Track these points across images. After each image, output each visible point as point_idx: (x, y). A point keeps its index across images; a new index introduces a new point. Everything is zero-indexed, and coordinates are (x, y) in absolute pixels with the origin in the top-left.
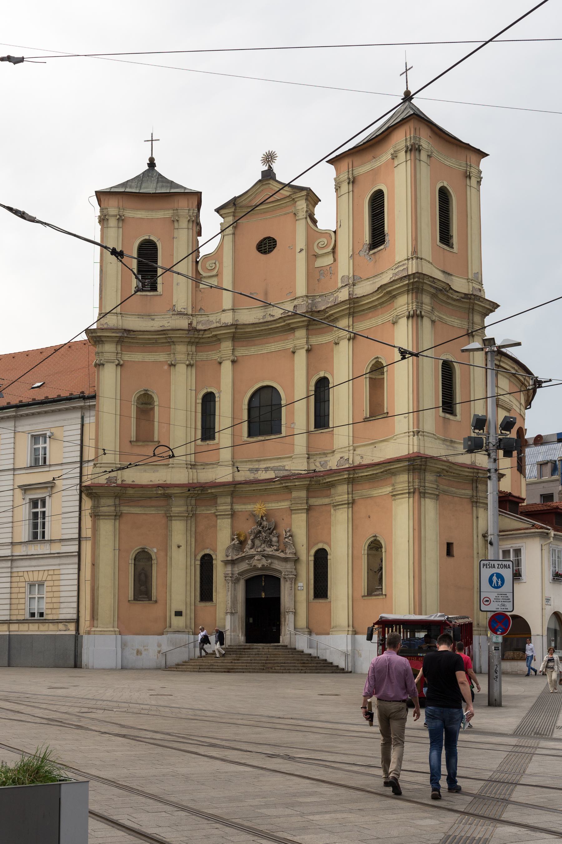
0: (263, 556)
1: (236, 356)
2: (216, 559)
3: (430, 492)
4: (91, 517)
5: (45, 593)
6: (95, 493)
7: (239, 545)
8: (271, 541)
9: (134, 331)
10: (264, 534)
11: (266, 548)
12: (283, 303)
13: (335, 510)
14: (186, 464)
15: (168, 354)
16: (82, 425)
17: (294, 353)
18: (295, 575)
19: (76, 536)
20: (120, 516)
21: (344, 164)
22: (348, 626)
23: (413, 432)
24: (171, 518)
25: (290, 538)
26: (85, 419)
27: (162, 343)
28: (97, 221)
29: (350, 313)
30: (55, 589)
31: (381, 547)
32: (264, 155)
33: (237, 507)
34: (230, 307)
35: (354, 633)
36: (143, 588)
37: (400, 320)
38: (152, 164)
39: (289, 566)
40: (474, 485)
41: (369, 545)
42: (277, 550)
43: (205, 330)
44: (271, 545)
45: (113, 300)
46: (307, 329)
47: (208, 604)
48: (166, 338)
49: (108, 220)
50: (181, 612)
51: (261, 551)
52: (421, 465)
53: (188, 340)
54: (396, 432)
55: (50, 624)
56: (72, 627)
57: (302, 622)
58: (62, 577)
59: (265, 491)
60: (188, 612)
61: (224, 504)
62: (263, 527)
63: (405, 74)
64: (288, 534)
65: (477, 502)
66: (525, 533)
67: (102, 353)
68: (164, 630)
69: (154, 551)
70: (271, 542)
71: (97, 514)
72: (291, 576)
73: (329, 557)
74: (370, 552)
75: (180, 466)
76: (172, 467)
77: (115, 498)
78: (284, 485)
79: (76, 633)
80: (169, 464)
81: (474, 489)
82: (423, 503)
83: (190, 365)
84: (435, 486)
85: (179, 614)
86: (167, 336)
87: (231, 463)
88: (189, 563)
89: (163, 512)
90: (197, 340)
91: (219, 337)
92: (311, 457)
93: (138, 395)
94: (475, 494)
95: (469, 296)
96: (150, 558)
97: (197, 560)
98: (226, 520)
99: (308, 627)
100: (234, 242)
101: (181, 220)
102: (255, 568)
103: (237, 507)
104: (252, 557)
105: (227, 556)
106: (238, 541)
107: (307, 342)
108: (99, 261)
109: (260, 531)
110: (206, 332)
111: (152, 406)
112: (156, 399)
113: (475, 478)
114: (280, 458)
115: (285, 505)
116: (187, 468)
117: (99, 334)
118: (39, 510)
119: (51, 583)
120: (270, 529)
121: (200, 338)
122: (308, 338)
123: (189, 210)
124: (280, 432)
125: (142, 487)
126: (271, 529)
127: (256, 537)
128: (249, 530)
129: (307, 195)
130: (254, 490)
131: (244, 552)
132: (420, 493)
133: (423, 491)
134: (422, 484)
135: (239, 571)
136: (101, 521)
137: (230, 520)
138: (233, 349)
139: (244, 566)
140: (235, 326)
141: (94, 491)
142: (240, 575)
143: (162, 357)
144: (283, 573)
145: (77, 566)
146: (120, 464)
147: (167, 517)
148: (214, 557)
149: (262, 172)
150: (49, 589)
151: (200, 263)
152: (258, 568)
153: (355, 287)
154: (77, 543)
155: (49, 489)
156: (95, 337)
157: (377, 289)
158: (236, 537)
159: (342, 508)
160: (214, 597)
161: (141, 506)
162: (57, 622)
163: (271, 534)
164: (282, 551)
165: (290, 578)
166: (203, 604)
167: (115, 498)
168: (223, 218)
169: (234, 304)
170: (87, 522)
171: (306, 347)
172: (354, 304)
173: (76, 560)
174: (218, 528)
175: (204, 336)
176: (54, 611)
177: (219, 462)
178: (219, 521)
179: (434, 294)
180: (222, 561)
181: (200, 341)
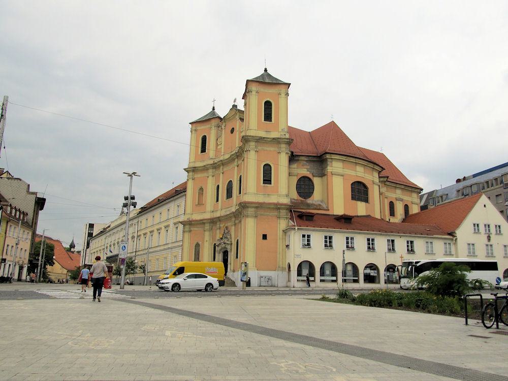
45: (193, 160)
69: (200, 243)
143: (205, 174)
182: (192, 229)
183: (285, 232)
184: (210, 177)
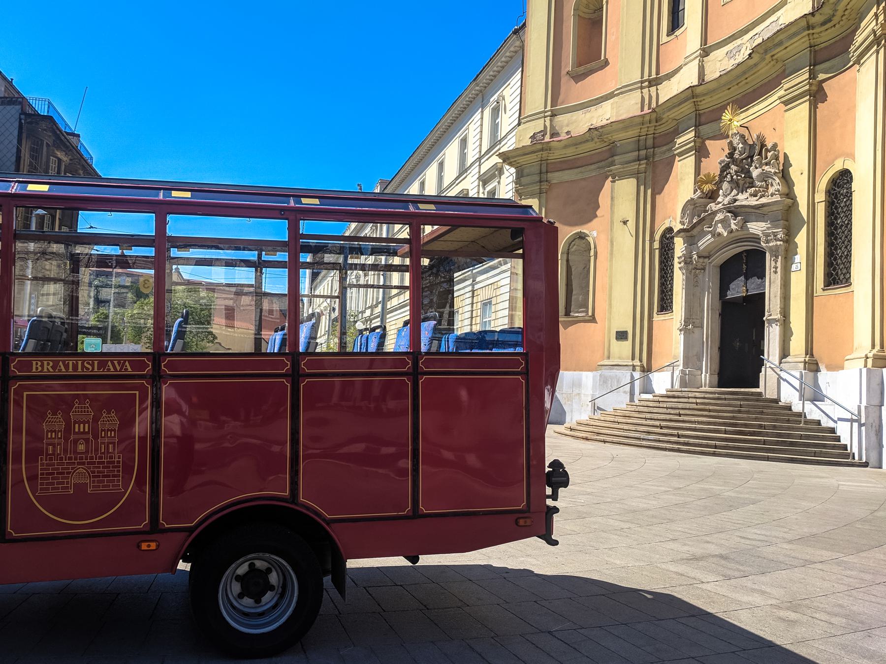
50: (626, 332)
85: (621, 336)
116: (642, 88)
166: (662, 317)
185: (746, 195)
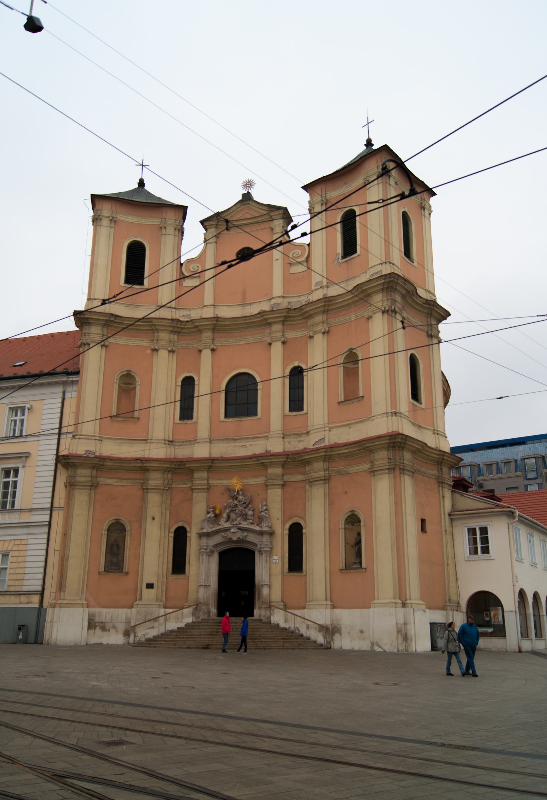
0: (238, 529)
1: (216, 346)
2: (190, 532)
3: (408, 469)
4: (66, 487)
5: (9, 563)
6: (73, 463)
7: (214, 518)
8: (246, 515)
9: (121, 317)
10: (240, 508)
11: (242, 522)
12: (260, 302)
13: (311, 486)
14: (165, 440)
15: (151, 340)
16: (63, 399)
17: (270, 344)
18: (271, 548)
19: (49, 506)
20: (96, 487)
21: (318, 189)
22: (326, 600)
23: (391, 413)
24: (147, 490)
25: (266, 511)
26: (66, 394)
27: (147, 330)
28: (91, 220)
29: (324, 310)
30: (20, 559)
31: (359, 521)
32: (244, 182)
33: (212, 482)
34: (211, 303)
35: (332, 606)
36: (114, 559)
37: (375, 315)
38: (141, 183)
39: (265, 538)
40: (439, 467)
41: (346, 520)
42: (252, 524)
43: (188, 321)
44: (246, 519)
46: (283, 324)
47: (181, 576)
48: (150, 325)
49: (101, 219)
51: (237, 524)
52: (401, 443)
53: (171, 329)
54: (373, 413)
55: (12, 597)
56: (36, 599)
57: (276, 595)
58: (29, 547)
59: (241, 467)
60: (160, 584)
61: (200, 478)
62: (239, 501)
63: (367, 126)
64: (265, 508)
65: (442, 483)
66: (492, 512)
67: (89, 333)
68: (135, 603)
70: (246, 516)
71: (73, 484)
72: (267, 549)
73: (304, 531)
74: (346, 526)
75: (158, 441)
76: (151, 443)
77: (92, 469)
78: (260, 461)
79: (40, 606)
80: (148, 440)
81: (440, 470)
82: (402, 479)
83: (171, 351)
84: (411, 464)
85: (150, 586)
86: (152, 324)
87: (208, 440)
88: (163, 535)
89: (139, 485)
90: (179, 330)
91: (200, 328)
92: (286, 437)
93: (121, 374)
94: (440, 475)
95: (430, 302)
96: (123, 529)
97: (171, 532)
98: (202, 494)
99: (283, 601)
100: (216, 249)
101: (168, 227)
102: (231, 541)
103: (212, 482)
104: (228, 530)
105: (202, 529)
106: (214, 514)
107: (283, 336)
108: (90, 253)
109: (236, 505)
110: (188, 323)
111: (132, 386)
112: (138, 379)
113: (441, 460)
114: (256, 438)
115: (259, 480)
116: (165, 444)
117: (86, 316)
118: (11, 479)
119: (16, 554)
120: (245, 503)
121: (182, 328)
122: (283, 332)
123: (176, 220)
124: (255, 414)
125: (121, 460)
126: (247, 504)
127: (232, 511)
128: (225, 504)
129: (283, 214)
130: (230, 466)
131: (219, 525)
132: (400, 469)
133: (402, 467)
134: (402, 461)
135: (214, 544)
136: (76, 490)
137: (205, 494)
138: (213, 339)
139: (218, 539)
140: (217, 318)
141: (71, 461)
142: (215, 547)
144: (259, 546)
145: (46, 536)
146: (99, 437)
147: (144, 489)
148: (188, 530)
149: (243, 194)
150: (15, 559)
151: (184, 266)
152: (233, 540)
153: (328, 289)
154: (49, 512)
155: (23, 459)
156: (83, 318)
157: (353, 287)
158: (211, 510)
159: (318, 484)
160: (187, 569)
161: (118, 478)
162: (20, 595)
163: (246, 508)
164: (258, 525)
165: (266, 551)
166: (175, 577)
167: (92, 469)
168: (206, 230)
169: (215, 302)
170: (61, 491)
171: (283, 339)
172: (329, 302)
173: (46, 530)
174: (194, 501)
175: (186, 327)
176: (17, 583)
177: (196, 440)
178: (194, 495)
179: (404, 295)
180: (197, 533)
181: (182, 331)
182: (101, 480)
183: (452, 520)
184: (163, 354)
185: (245, 523)
